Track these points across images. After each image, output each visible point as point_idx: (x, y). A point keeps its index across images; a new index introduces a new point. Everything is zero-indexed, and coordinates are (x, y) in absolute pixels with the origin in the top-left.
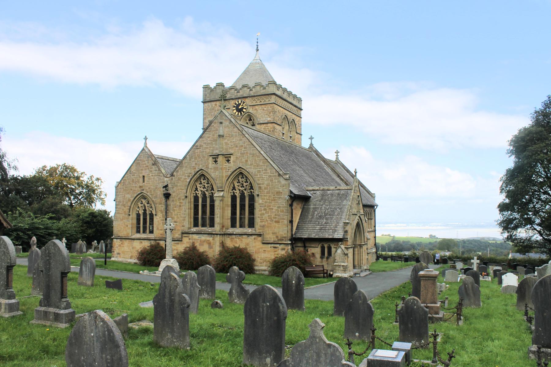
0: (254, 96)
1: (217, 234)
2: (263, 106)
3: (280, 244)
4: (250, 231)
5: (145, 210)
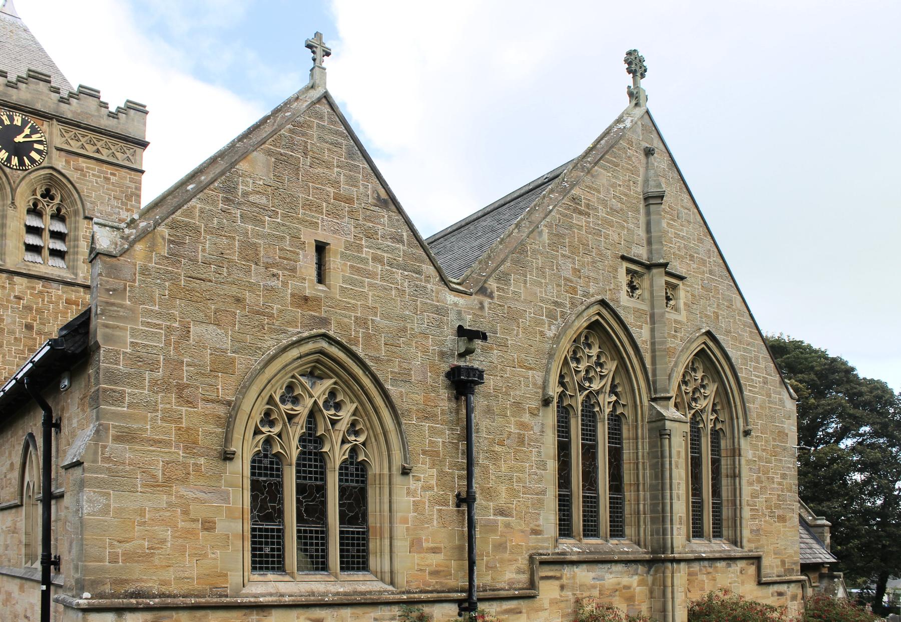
1: (679, 561)
2: (105, 167)
3: (789, 582)
4: (721, 546)
5: (312, 441)
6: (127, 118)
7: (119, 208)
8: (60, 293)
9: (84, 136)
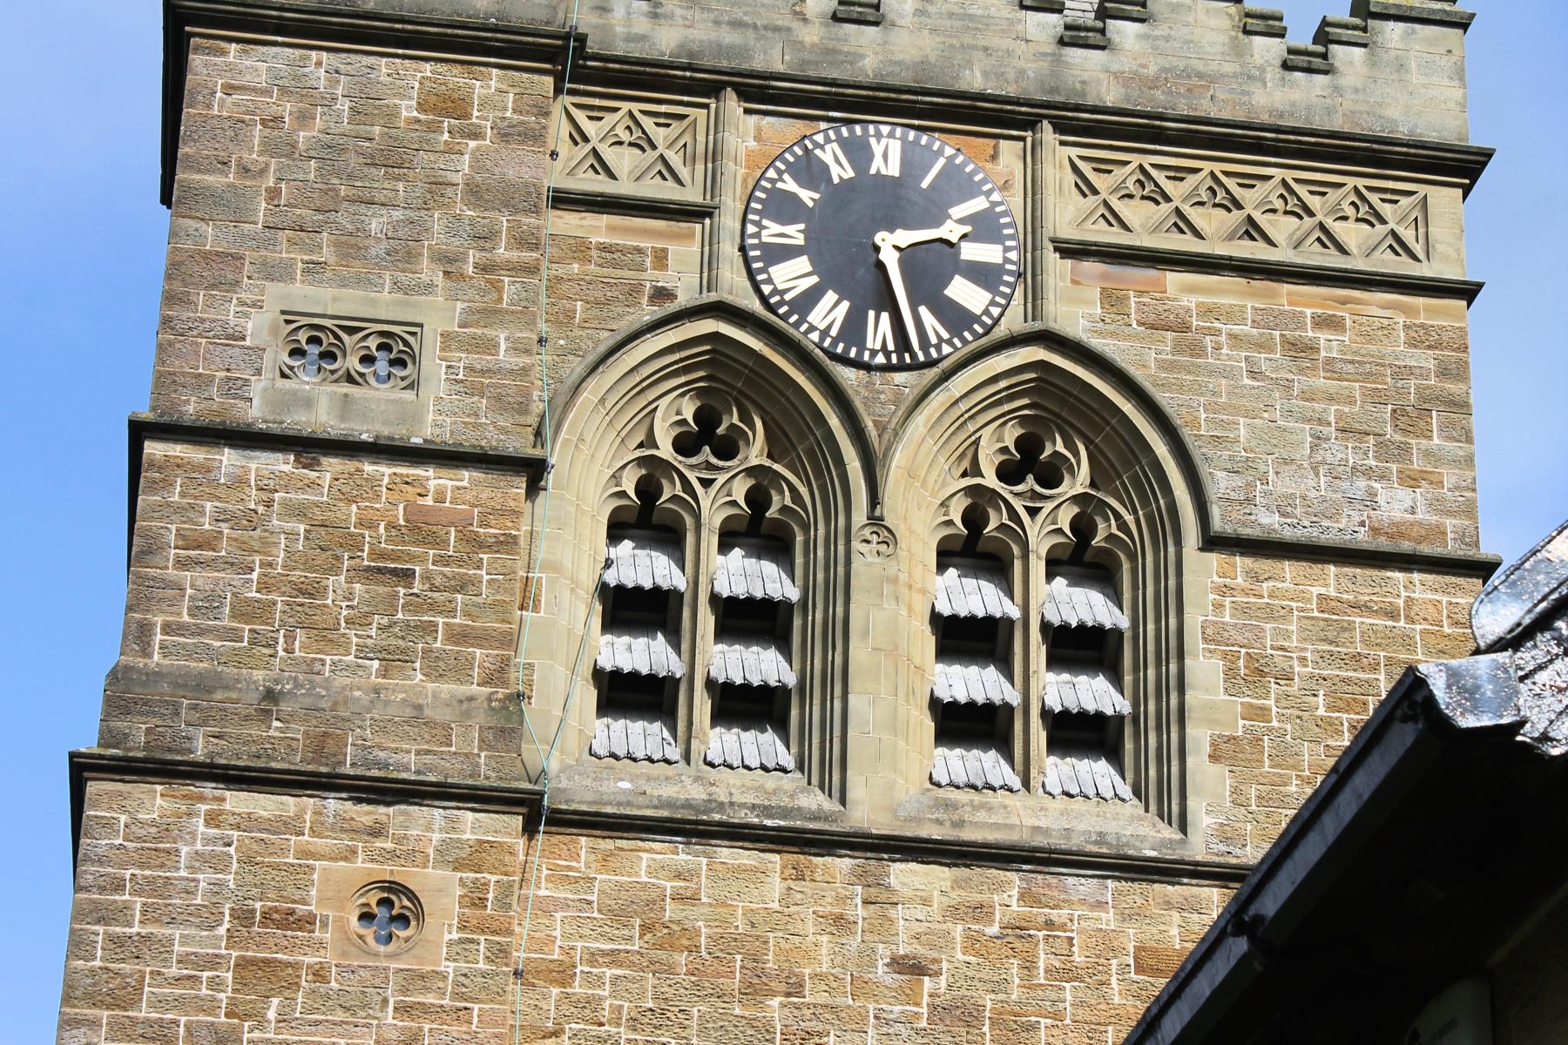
6: (1373, 62)
7: (1368, 473)
8: (1108, 919)
9: (1178, 174)
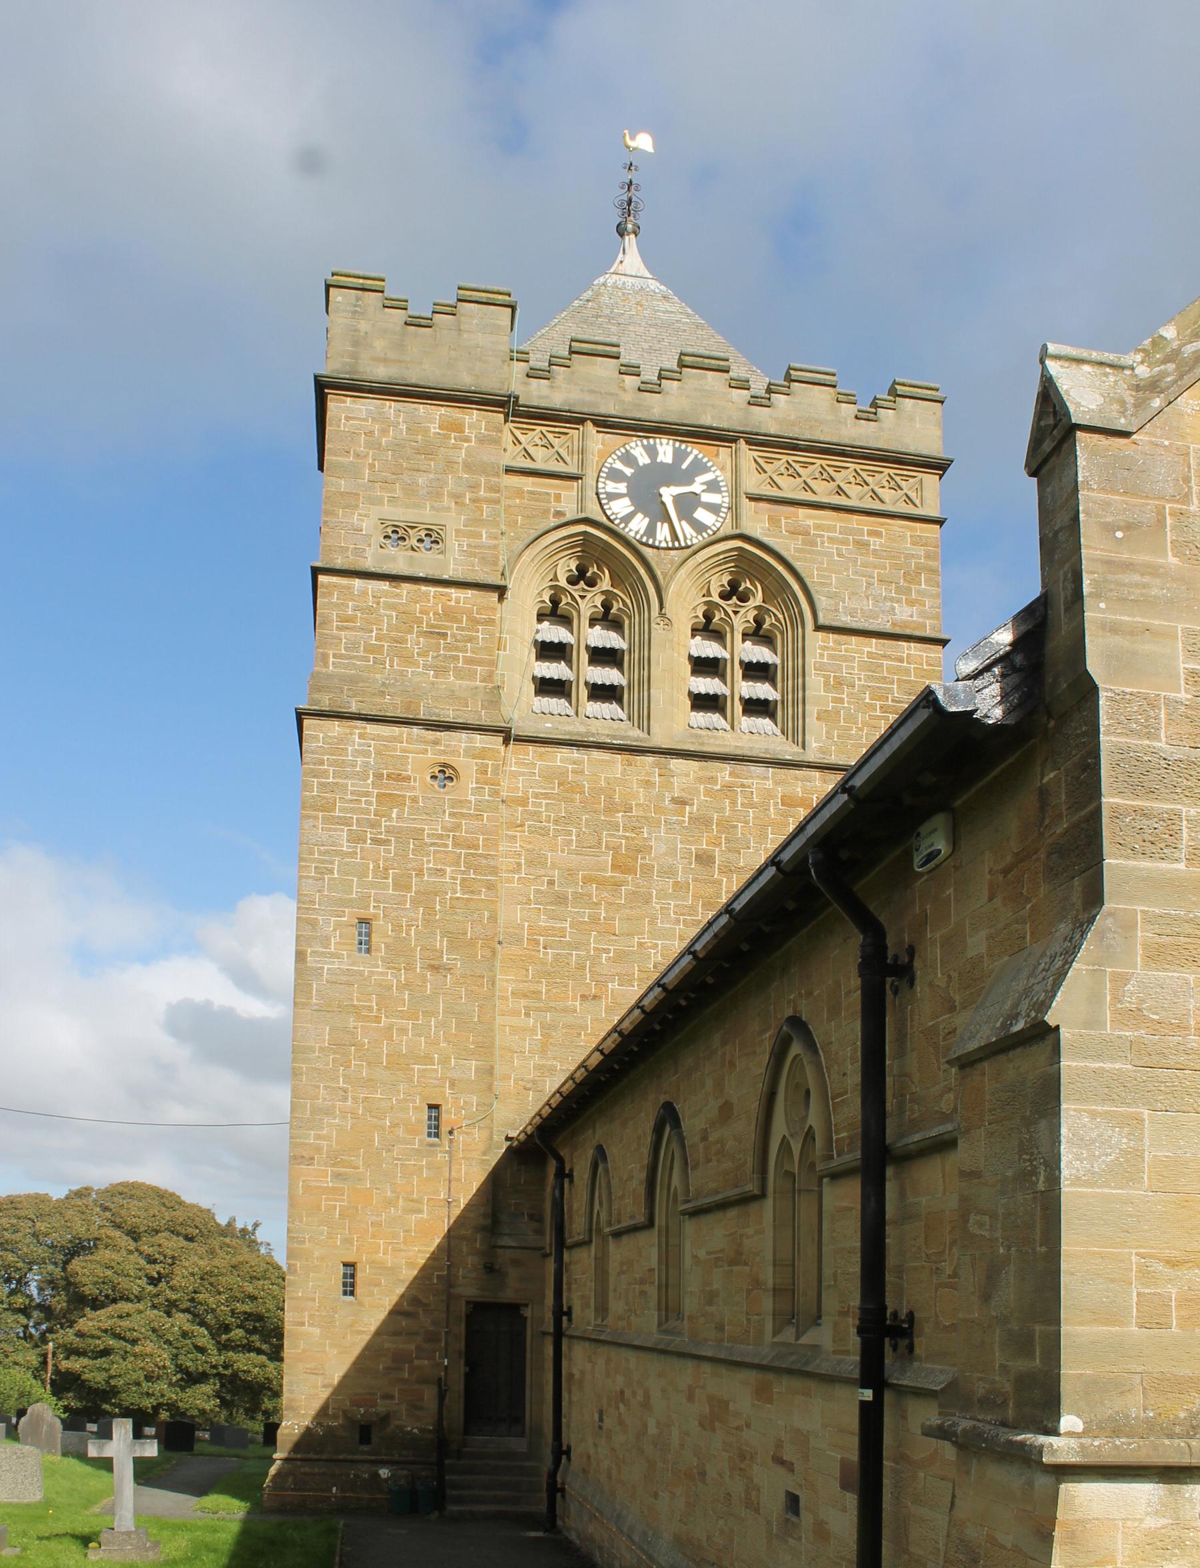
0: (791, 446)
7: (892, 599)
8: (769, 784)
9: (805, 465)
